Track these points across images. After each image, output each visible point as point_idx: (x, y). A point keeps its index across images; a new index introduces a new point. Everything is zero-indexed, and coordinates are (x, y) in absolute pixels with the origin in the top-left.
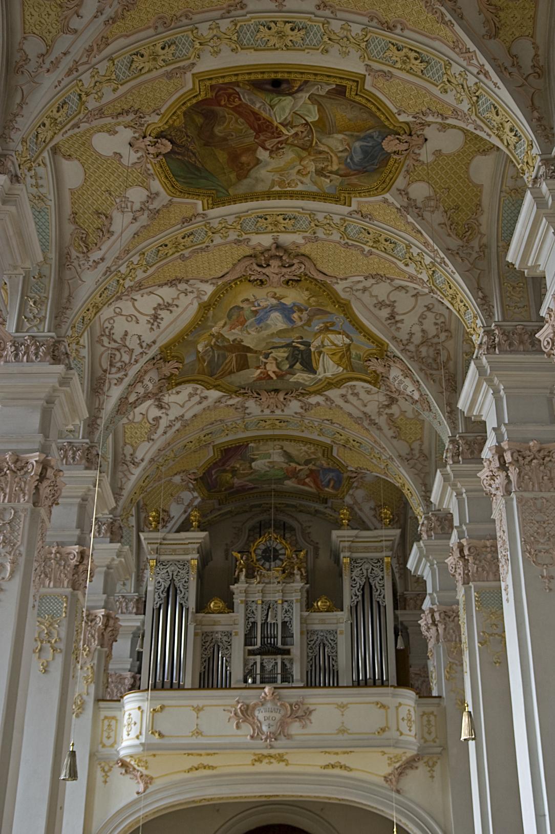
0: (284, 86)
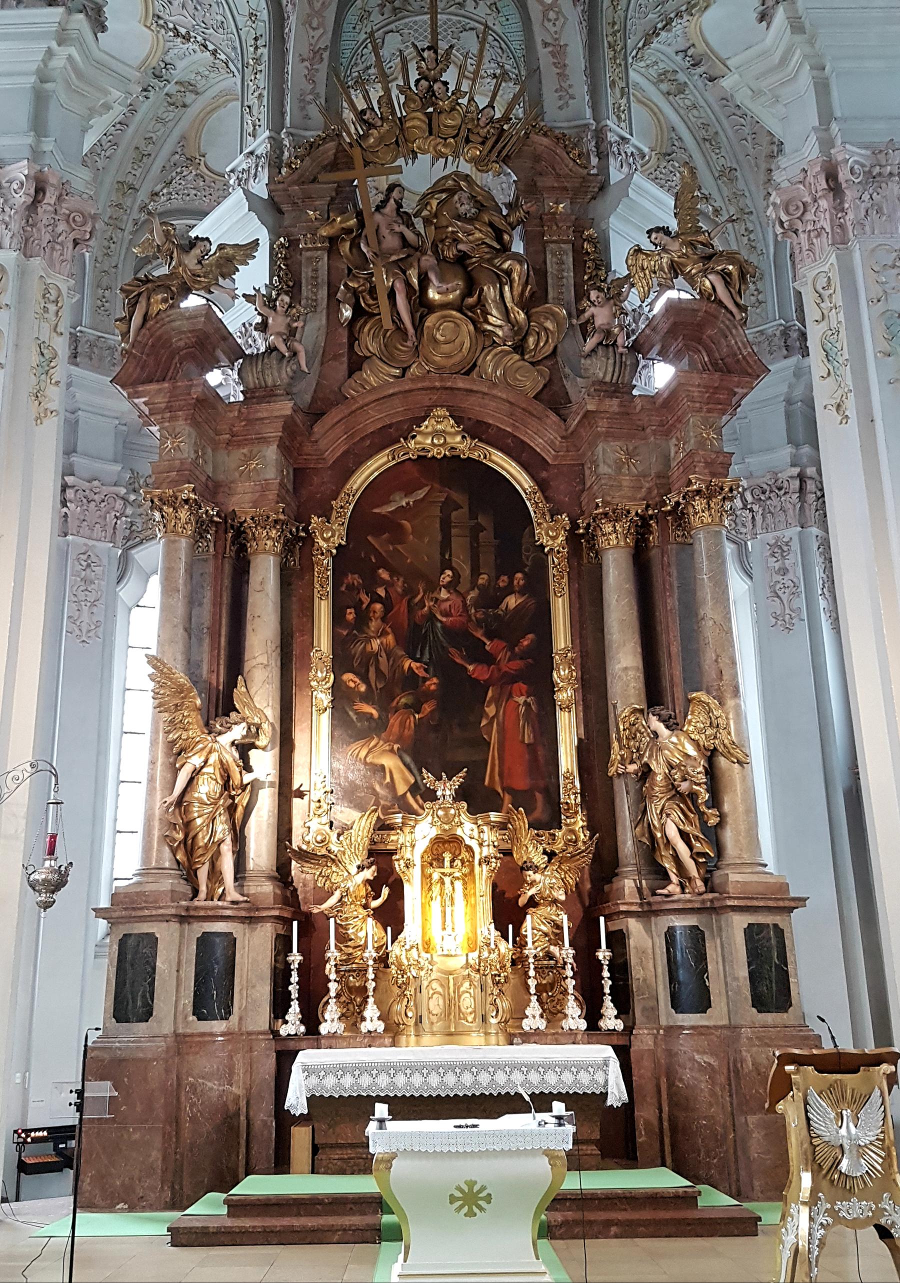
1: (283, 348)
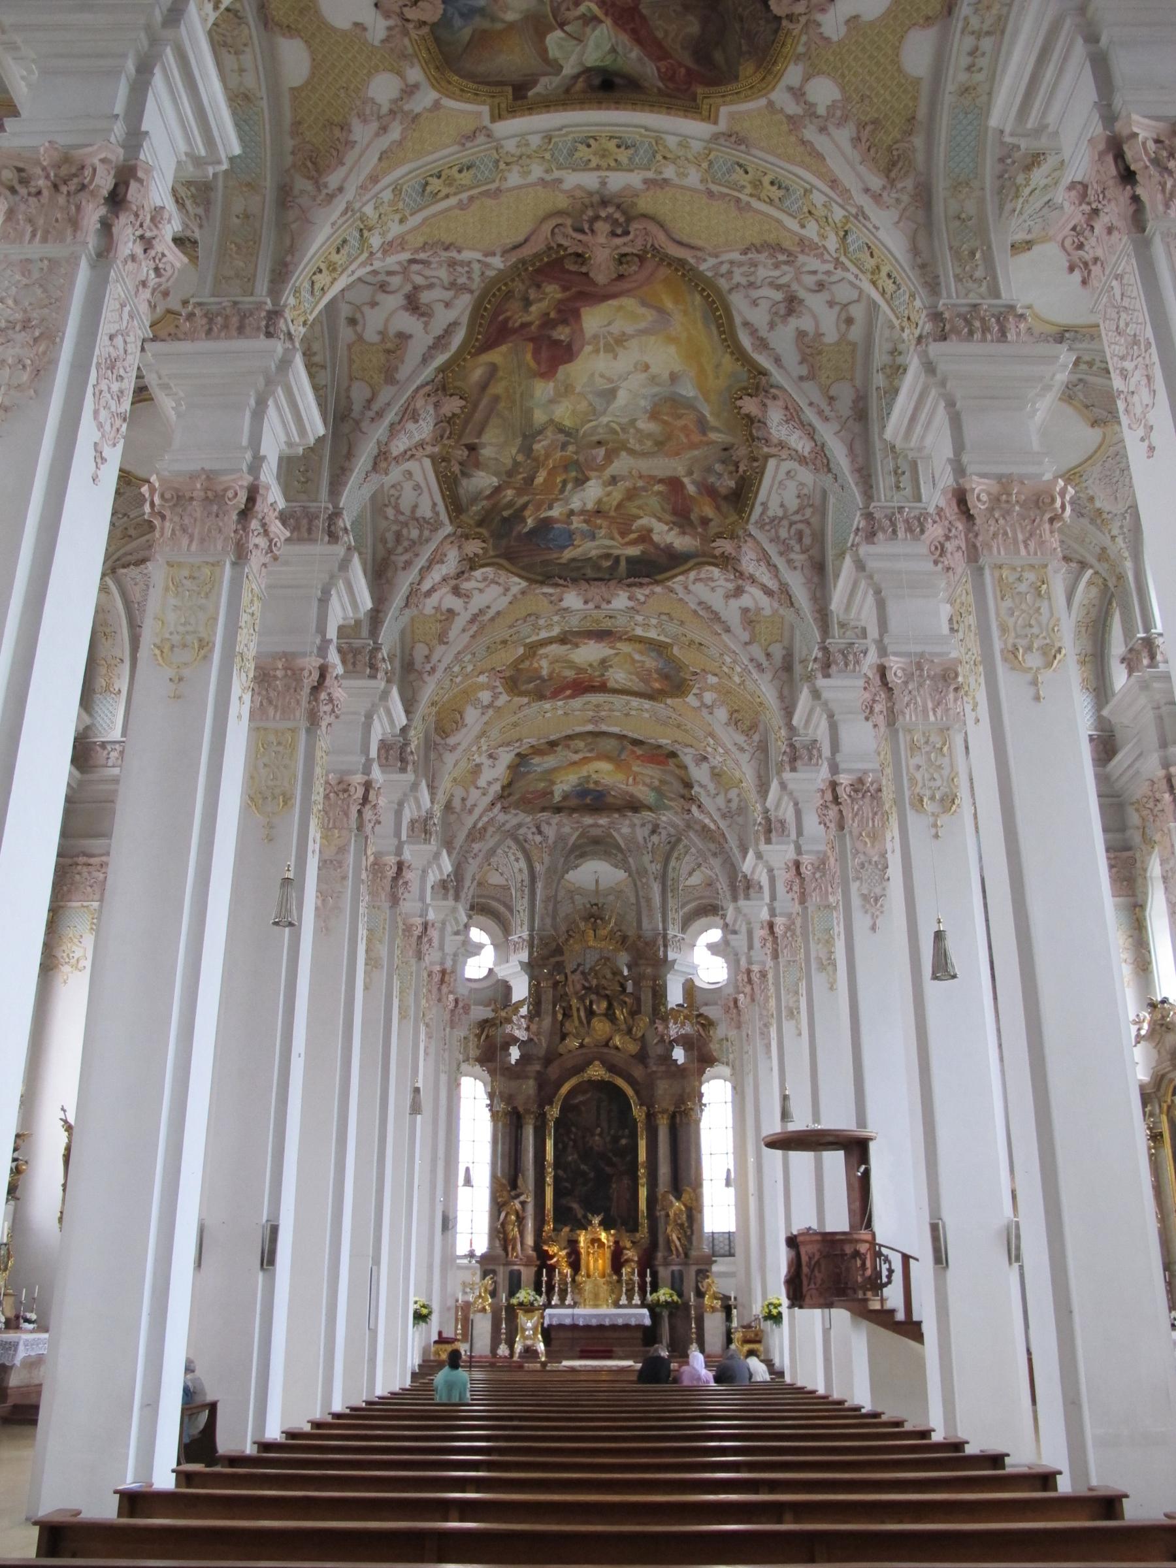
0: (597, 81)
1: (535, 1039)
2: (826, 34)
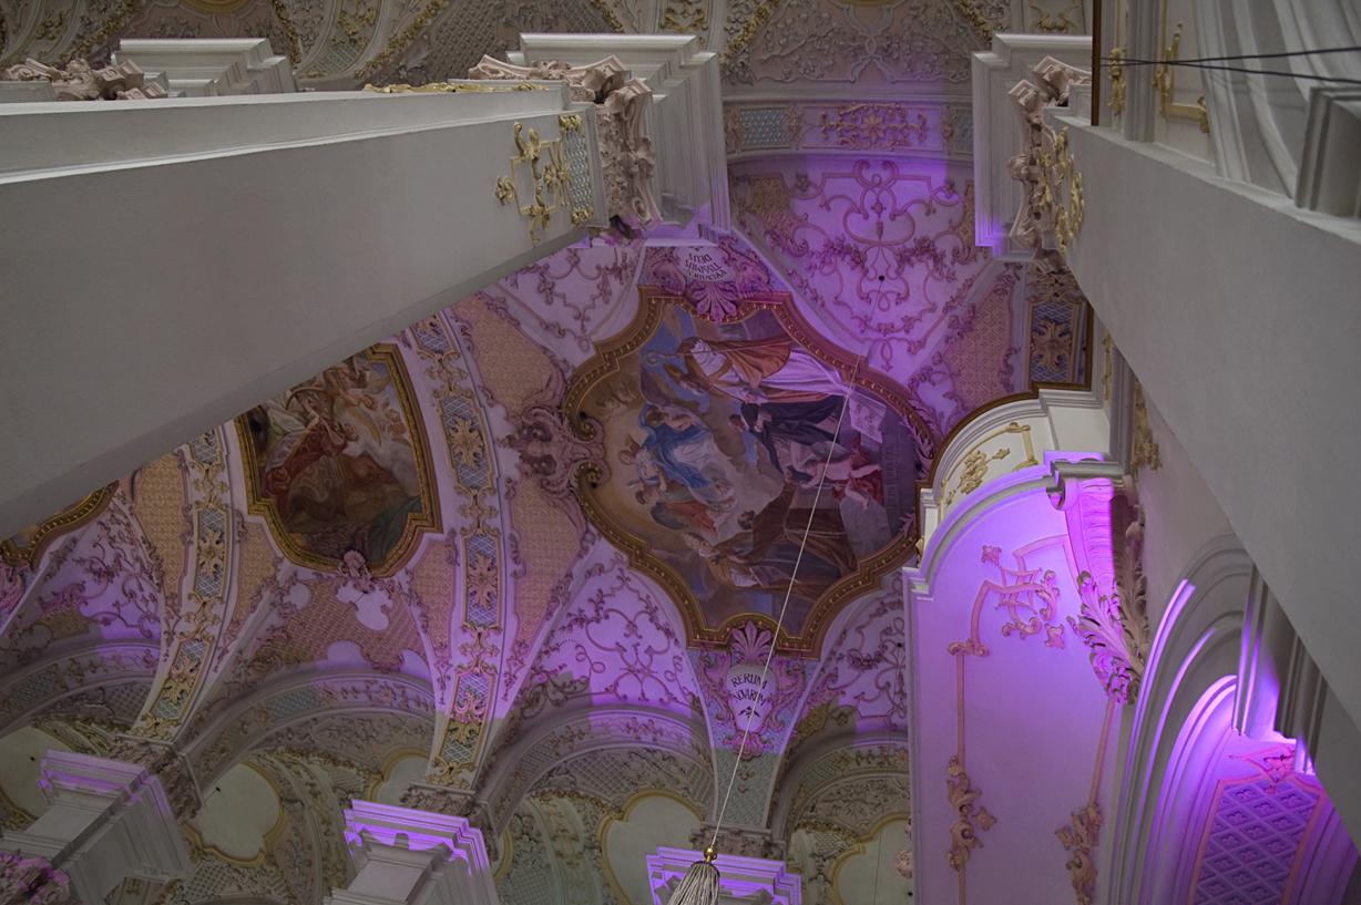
2: (340, 591)
